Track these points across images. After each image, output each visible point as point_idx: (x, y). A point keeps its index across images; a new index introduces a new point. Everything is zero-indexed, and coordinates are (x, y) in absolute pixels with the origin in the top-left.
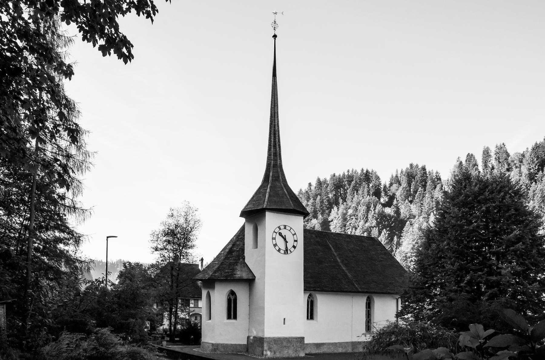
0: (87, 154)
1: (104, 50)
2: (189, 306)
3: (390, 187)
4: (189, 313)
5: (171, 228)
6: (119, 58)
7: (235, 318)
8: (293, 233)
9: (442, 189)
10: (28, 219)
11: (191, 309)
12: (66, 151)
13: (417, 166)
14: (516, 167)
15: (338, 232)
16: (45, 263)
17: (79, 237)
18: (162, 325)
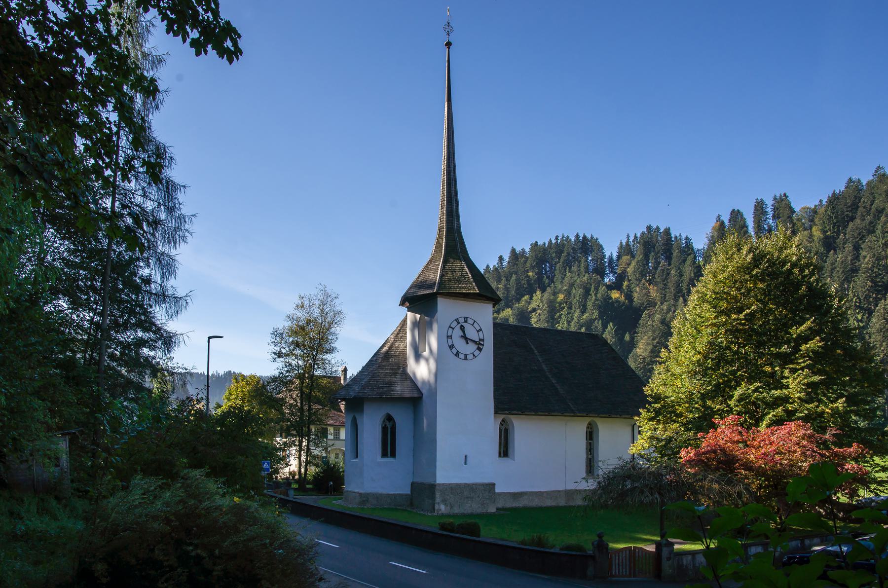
0: (181, 218)
1: (198, 47)
2: (327, 437)
3: (617, 260)
4: (326, 449)
5: (301, 323)
6: (221, 55)
7: (393, 455)
8: (478, 328)
9: (694, 263)
10: (101, 314)
11: (330, 443)
12: (153, 215)
13: (658, 228)
14: (805, 229)
15: (542, 326)
16: (122, 376)
17: (171, 337)
18: (287, 465)
